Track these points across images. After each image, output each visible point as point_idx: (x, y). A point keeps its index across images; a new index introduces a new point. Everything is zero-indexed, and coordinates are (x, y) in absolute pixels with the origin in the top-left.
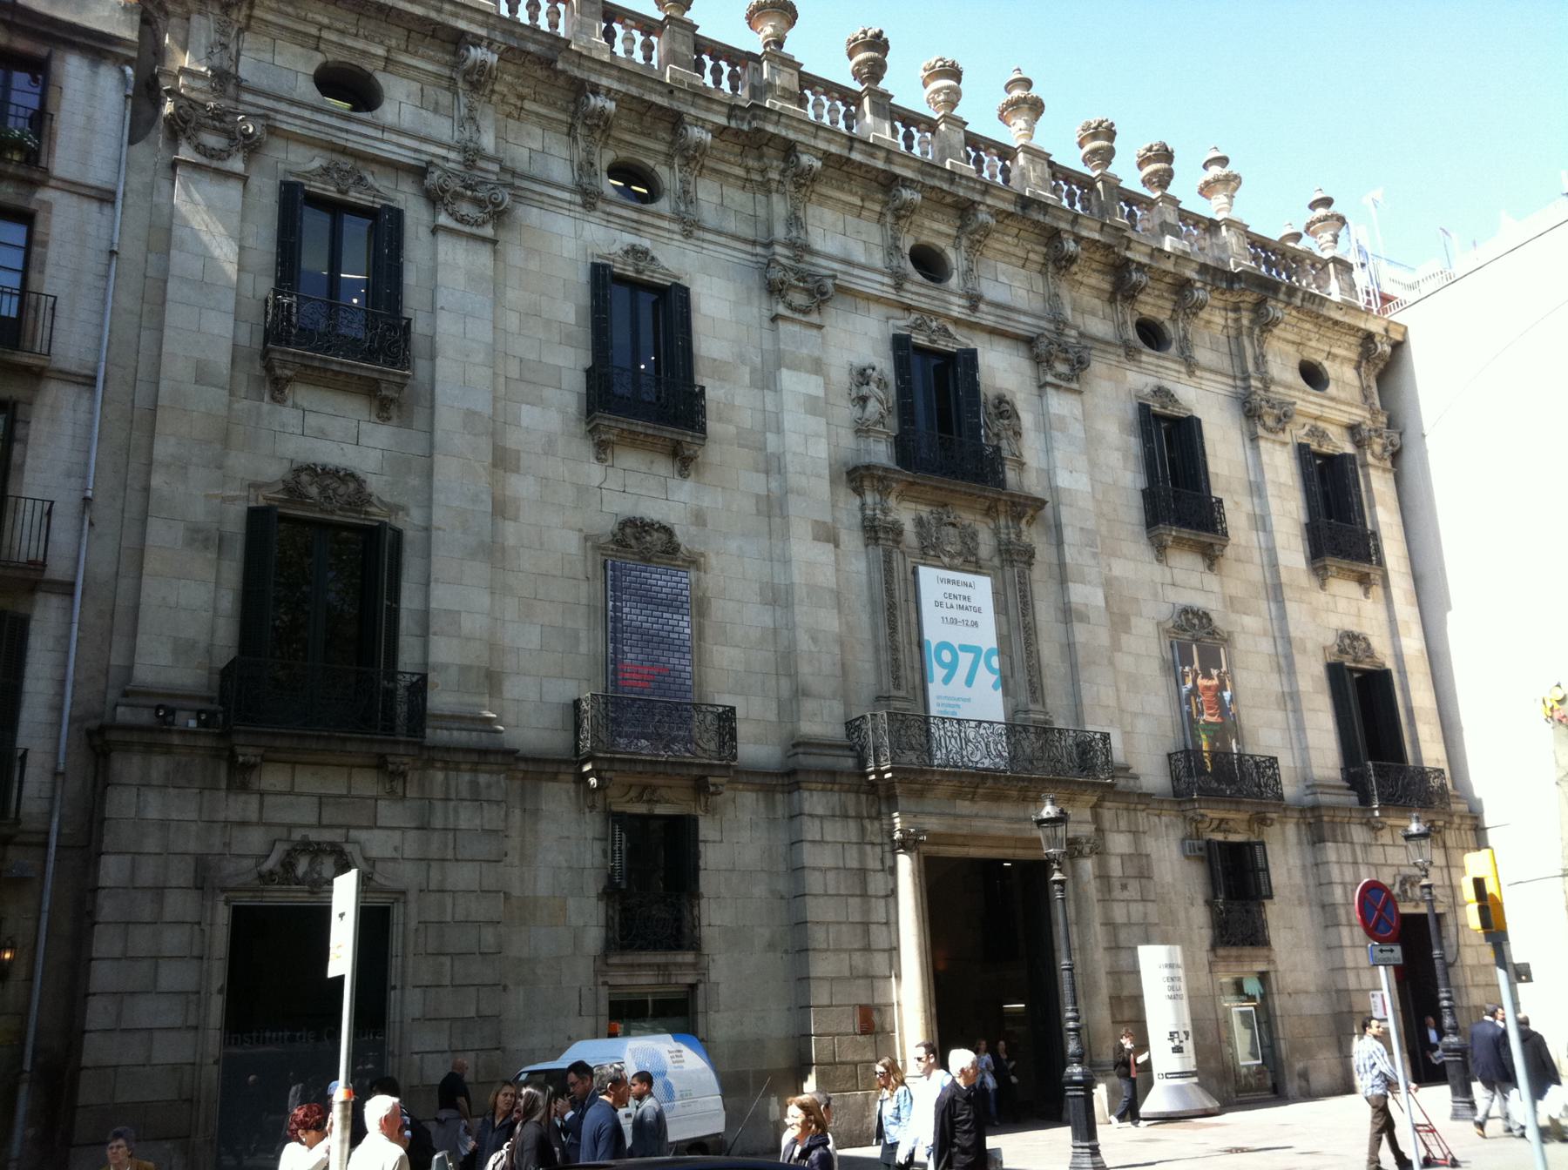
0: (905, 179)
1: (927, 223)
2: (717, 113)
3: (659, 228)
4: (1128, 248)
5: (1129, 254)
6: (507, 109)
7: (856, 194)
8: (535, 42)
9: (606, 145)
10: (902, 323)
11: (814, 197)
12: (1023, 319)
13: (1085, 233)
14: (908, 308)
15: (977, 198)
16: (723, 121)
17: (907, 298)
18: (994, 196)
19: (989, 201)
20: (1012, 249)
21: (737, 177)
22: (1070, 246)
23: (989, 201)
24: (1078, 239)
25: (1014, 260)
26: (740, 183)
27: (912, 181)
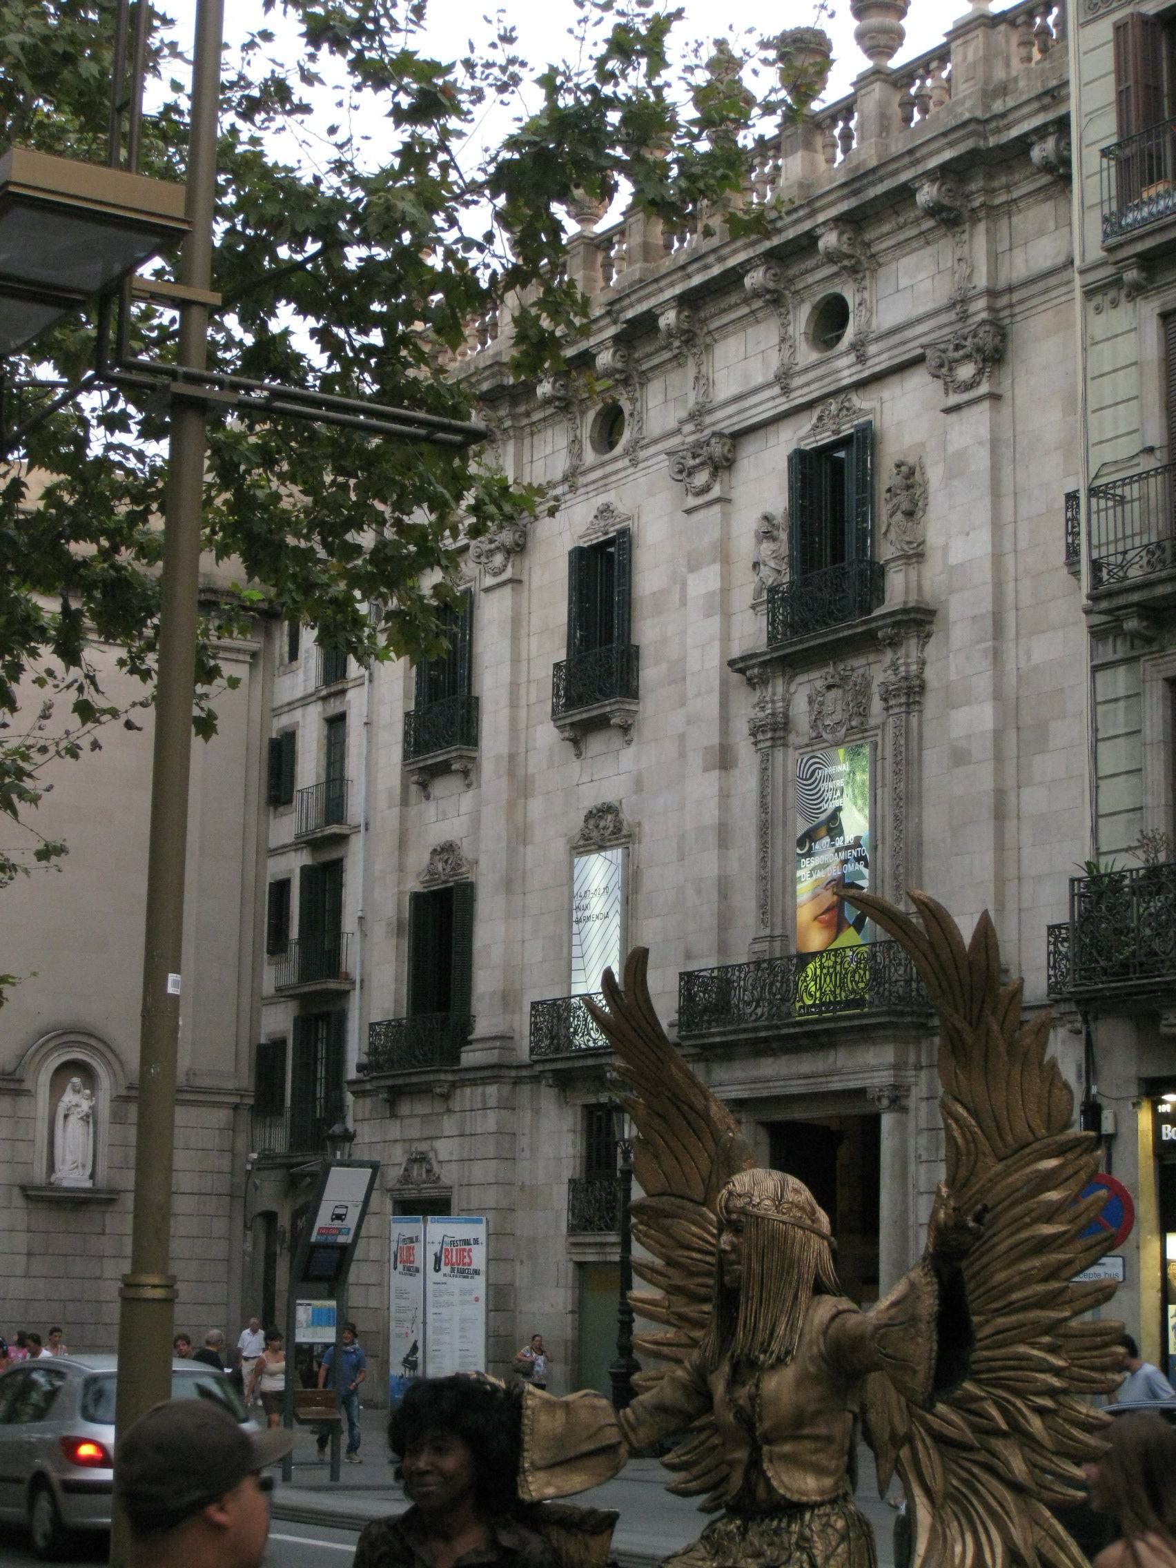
0: (741, 265)
1: (810, 279)
2: (607, 327)
3: (616, 472)
4: (1008, 127)
5: (1014, 133)
6: (528, 430)
7: (737, 305)
8: (486, 379)
9: (588, 408)
10: (809, 427)
11: (716, 336)
12: (920, 329)
13: (933, 163)
14: (810, 405)
15: (807, 226)
16: (612, 331)
17: (799, 398)
18: (823, 209)
19: (821, 218)
20: (902, 236)
21: (670, 360)
22: (927, 194)
23: (821, 218)
24: (931, 175)
25: (914, 244)
26: (675, 363)
27: (748, 261)
